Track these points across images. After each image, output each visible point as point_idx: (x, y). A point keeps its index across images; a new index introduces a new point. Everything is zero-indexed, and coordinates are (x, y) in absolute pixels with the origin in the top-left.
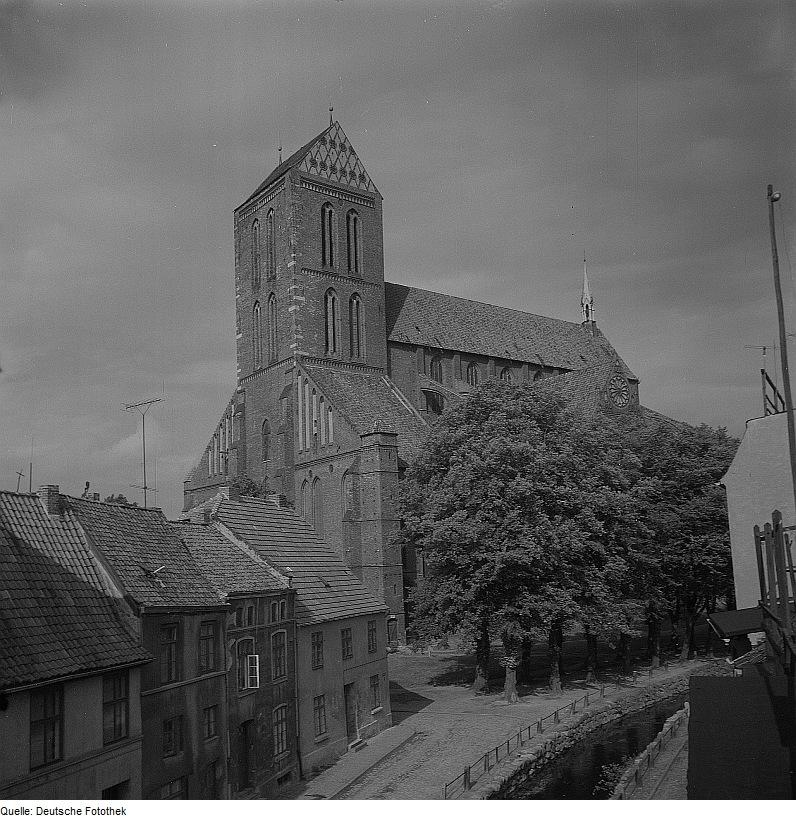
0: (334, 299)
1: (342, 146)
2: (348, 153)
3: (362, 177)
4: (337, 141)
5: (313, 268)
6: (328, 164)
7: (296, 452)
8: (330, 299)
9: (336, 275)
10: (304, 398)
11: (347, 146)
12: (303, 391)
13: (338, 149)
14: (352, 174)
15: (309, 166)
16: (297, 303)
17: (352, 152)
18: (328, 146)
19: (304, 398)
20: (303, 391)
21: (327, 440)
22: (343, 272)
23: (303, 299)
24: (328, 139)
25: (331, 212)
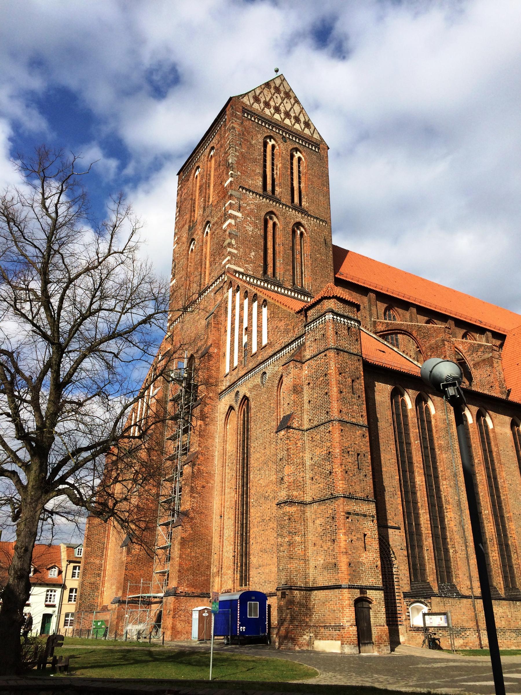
0: (274, 224)
1: (288, 95)
2: (292, 101)
3: (307, 124)
4: (281, 88)
5: (252, 189)
6: (272, 103)
7: (222, 375)
8: (270, 224)
9: (278, 201)
10: (233, 309)
11: (291, 94)
12: (233, 302)
13: (282, 95)
14: (297, 120)
15: (252, 101)
16: (231, 216)
17: (297, 101)
18: (273, 91)
19: (233, 309)
20: (233, 302)
21: (259, 342)
22: (286, 199)
23: (239, 215)
24: (273, 85)
25: (273, 147)
